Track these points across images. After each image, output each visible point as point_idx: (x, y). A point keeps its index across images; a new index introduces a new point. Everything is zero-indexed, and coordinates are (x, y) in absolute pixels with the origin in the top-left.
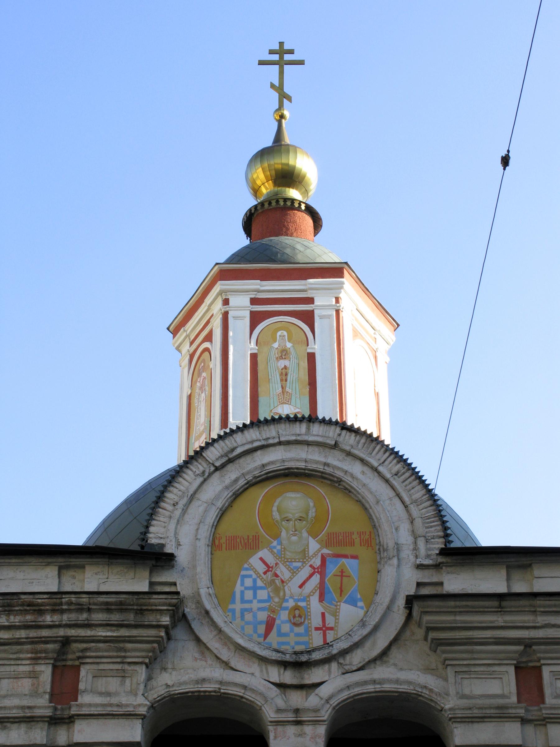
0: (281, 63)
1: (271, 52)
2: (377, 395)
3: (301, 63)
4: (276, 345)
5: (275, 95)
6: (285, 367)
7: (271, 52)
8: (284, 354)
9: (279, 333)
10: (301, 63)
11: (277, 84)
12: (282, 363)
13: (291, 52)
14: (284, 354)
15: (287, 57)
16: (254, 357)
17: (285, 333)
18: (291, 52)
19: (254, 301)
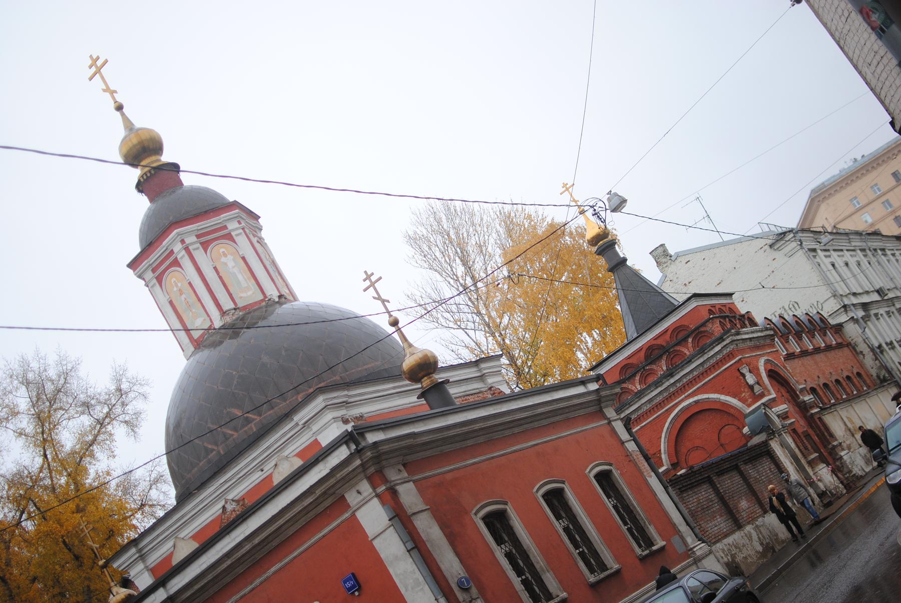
0: (98, 71)
1: (90, 67)
2: (244, 258)
3: (106, 62)
4: (175, 289)
5: (108, 95)
6: (185, 299)
7: (90, 67)
8: (181, 292)
9: (172, 282)
10: (106, 62)
11: (105, 88)
12: (183, 296)
13: (98, 58)
14: (181, 292)
15: (99, 63)
16: (171, 303)
17: (175, 279)
18: (98, 58)
19: (154, 271)
